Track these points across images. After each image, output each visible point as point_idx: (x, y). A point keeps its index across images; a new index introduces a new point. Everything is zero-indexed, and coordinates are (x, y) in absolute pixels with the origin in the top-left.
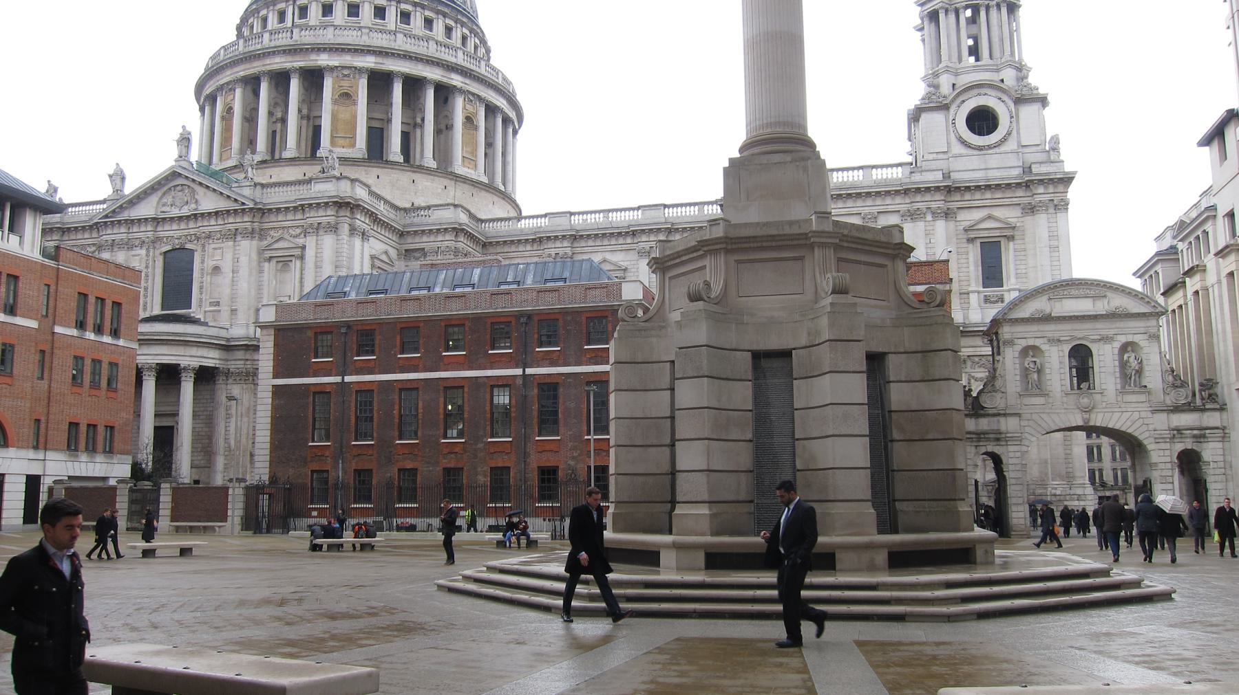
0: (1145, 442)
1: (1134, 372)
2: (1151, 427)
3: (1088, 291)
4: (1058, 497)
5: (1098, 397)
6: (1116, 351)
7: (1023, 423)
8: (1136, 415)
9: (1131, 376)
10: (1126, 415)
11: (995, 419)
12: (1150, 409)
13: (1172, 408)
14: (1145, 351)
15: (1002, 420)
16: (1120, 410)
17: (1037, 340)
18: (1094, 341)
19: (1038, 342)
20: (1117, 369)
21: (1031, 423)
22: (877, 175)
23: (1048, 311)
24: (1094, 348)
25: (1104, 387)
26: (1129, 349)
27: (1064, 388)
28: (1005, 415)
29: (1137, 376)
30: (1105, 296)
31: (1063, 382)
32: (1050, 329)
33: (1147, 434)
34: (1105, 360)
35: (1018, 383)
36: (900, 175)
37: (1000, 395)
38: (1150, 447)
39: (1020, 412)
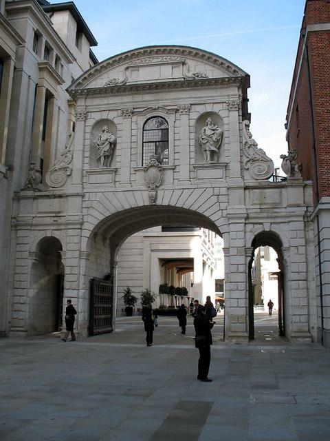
5: (169, 173)
6: (193, 122)
9: (211, 153)
14: (226, 121)
19: (110, 115)
24: (171, 119)
27: (134, 165)
32: (127, 100)
34: (182, 130)
35: (87, 160)
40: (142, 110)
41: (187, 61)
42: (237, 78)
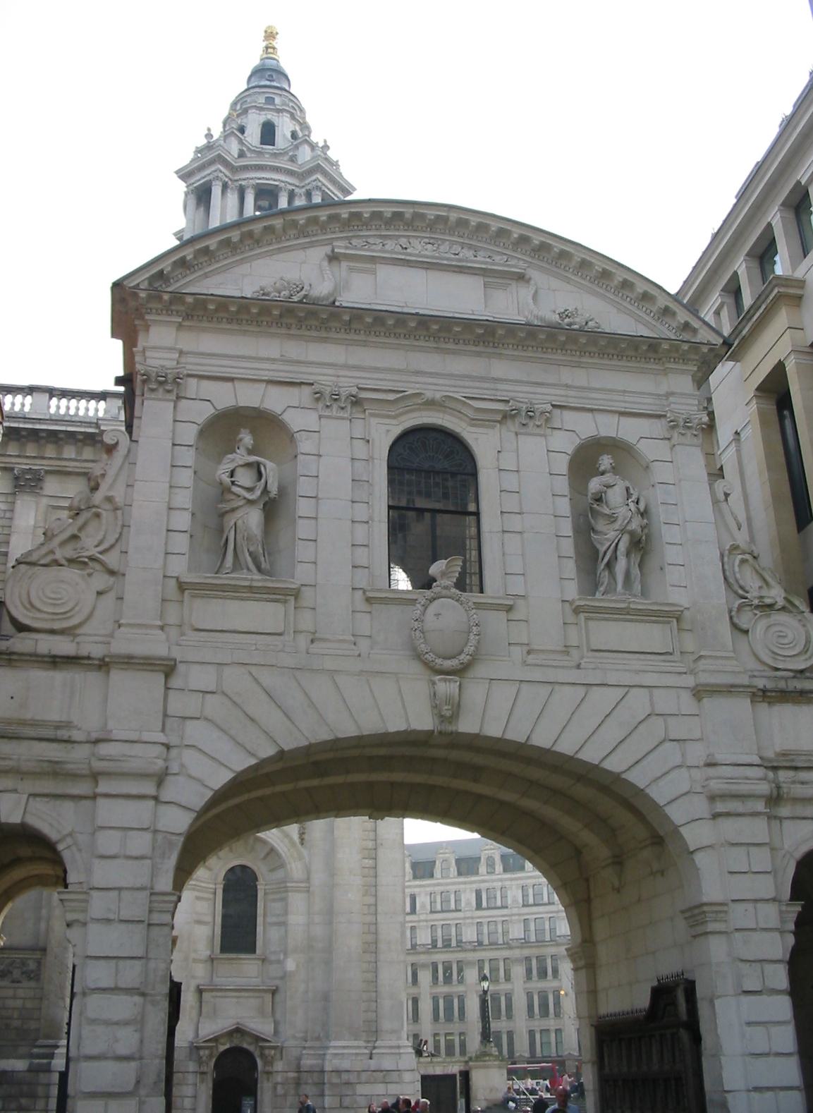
0: (676, 814)
1: (626, 539)
2: (697, 753)
3: (468, 254)
4: (345, 1077)
5: (495, 622)
6: (562, 464)
7: (178, 704)
8: (638, 703)
10: (603, 699)
11: (59, 677)
12: (690, 681)
13: (760, 683)
14: (662, 473)
15: (86, 680)
16: (573, 676)
17: (274, 391)
18: (483, 420)
19: (274, 401)
20: (567, 528)
21: (214, 706)
22: (58, 407)
23: (321, 288)
25: (517, 586)
26: (606, 461)
27: (362, 580)
28: (103, 665)
29: (635, 558)
30: (521, 278)
31: (362, 556)
33: (681, 781)
35: (181, 543)
36: (101, 414)
37: (101, 581)
38: (695, 835)
39: (177, 653)
40: (391, 397)
41: (533, 274)
42: (695, 346)
